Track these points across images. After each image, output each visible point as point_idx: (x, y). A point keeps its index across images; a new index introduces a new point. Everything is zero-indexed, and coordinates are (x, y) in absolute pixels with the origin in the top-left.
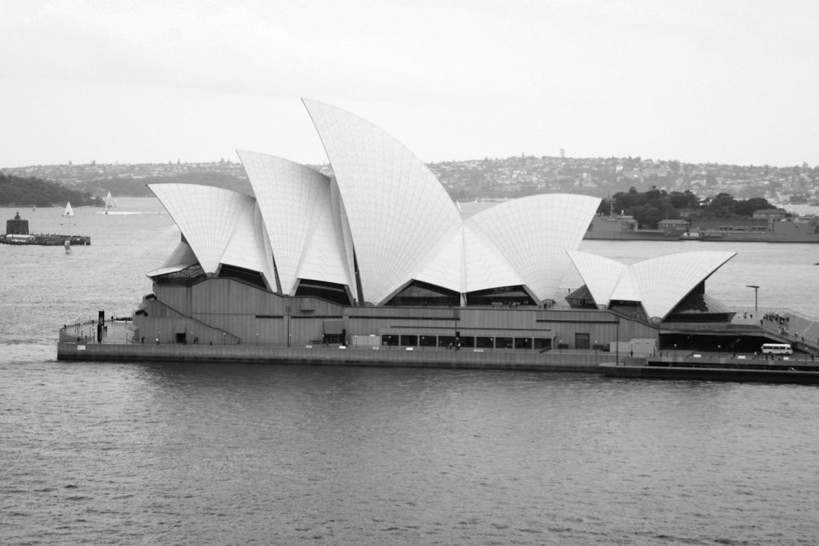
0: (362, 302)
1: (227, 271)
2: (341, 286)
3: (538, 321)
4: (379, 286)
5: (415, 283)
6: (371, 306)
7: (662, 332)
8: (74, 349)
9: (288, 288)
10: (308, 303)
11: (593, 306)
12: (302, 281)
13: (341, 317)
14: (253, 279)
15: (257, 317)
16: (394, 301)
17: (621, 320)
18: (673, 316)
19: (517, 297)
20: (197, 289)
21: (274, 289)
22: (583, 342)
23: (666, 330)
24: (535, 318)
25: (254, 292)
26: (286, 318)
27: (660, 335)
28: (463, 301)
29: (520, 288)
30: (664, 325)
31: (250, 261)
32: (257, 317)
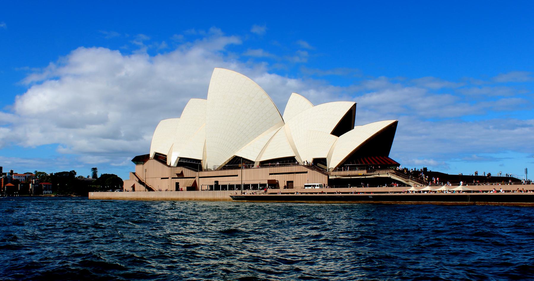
2: (199, 161)
3: (270, 174)
6: (211, 170)
7: (330, 178)
10: (179, 170)
13: (195, 178)
15: (162, 178)
17: (309, 170)
18: (341, 166)
21: (168, 164)
22: (290, 185)
23: (332, 176)
24: (269, 173)
25: (160, 164)
27: (328, 179)
28: (256, 165)
32: (162, 178)
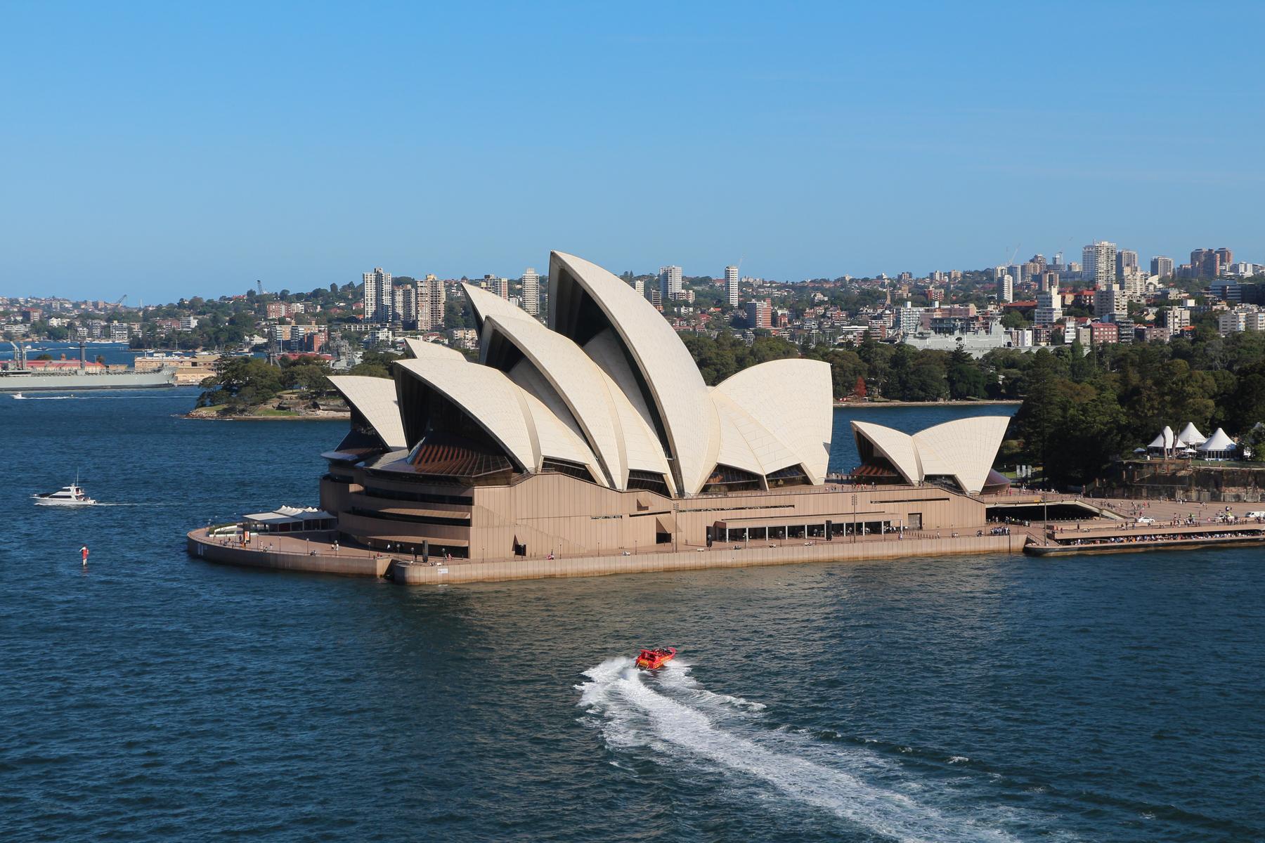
0: (681, 492)
1: (553, 465)
4: (695, 475)
5: (721, 469)
8: (434, 574)
9: (621, 481)
10: (646, 496)
11: (899, 479)
12: (633, 473)
14: (579, 472)
16: (705, 489)
18: (989, 488)
19: (793, 476)
20: (523, 488)
26: (626, 517)
29: (798, 468)
30: (986, 498)
31: (576, 452)
